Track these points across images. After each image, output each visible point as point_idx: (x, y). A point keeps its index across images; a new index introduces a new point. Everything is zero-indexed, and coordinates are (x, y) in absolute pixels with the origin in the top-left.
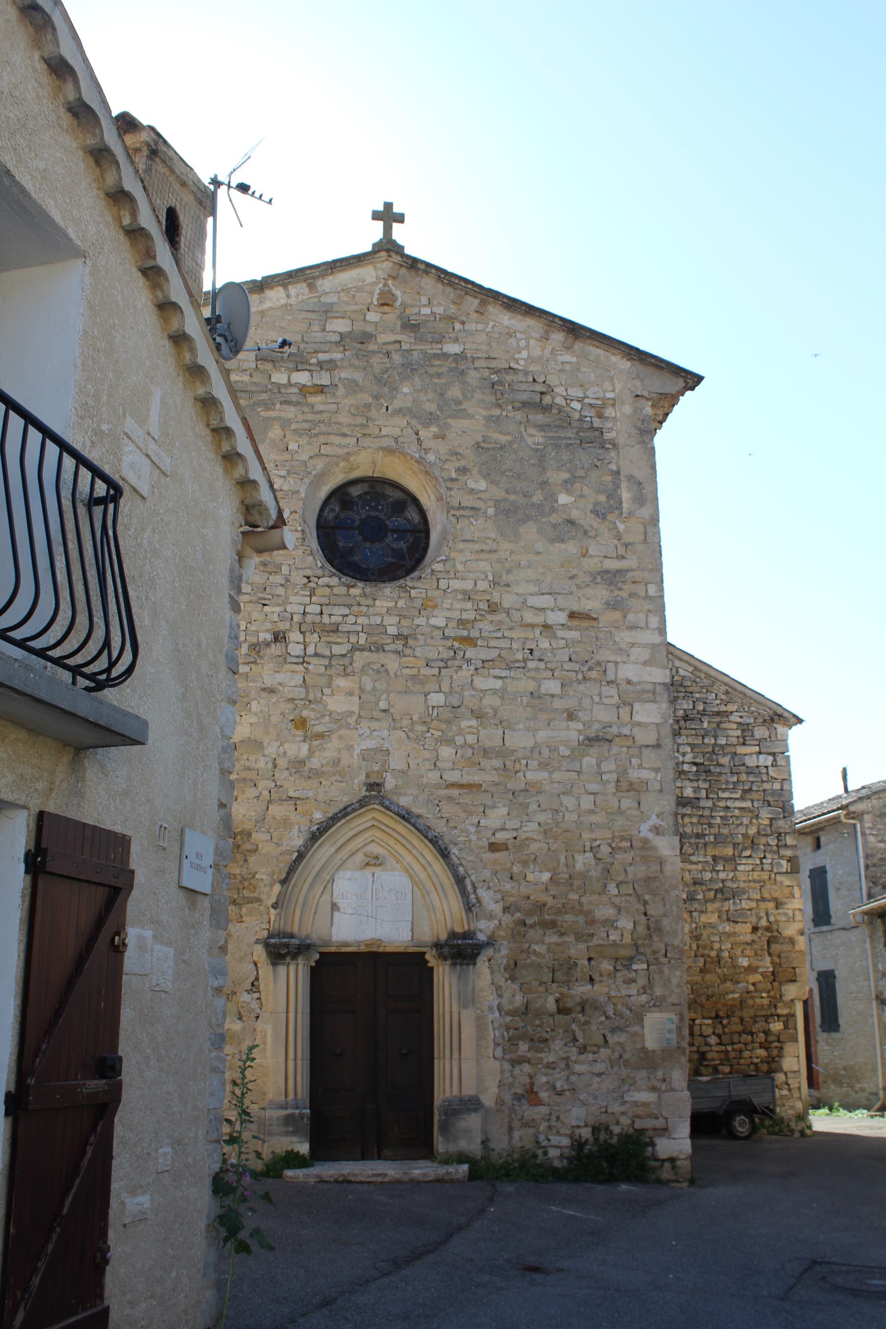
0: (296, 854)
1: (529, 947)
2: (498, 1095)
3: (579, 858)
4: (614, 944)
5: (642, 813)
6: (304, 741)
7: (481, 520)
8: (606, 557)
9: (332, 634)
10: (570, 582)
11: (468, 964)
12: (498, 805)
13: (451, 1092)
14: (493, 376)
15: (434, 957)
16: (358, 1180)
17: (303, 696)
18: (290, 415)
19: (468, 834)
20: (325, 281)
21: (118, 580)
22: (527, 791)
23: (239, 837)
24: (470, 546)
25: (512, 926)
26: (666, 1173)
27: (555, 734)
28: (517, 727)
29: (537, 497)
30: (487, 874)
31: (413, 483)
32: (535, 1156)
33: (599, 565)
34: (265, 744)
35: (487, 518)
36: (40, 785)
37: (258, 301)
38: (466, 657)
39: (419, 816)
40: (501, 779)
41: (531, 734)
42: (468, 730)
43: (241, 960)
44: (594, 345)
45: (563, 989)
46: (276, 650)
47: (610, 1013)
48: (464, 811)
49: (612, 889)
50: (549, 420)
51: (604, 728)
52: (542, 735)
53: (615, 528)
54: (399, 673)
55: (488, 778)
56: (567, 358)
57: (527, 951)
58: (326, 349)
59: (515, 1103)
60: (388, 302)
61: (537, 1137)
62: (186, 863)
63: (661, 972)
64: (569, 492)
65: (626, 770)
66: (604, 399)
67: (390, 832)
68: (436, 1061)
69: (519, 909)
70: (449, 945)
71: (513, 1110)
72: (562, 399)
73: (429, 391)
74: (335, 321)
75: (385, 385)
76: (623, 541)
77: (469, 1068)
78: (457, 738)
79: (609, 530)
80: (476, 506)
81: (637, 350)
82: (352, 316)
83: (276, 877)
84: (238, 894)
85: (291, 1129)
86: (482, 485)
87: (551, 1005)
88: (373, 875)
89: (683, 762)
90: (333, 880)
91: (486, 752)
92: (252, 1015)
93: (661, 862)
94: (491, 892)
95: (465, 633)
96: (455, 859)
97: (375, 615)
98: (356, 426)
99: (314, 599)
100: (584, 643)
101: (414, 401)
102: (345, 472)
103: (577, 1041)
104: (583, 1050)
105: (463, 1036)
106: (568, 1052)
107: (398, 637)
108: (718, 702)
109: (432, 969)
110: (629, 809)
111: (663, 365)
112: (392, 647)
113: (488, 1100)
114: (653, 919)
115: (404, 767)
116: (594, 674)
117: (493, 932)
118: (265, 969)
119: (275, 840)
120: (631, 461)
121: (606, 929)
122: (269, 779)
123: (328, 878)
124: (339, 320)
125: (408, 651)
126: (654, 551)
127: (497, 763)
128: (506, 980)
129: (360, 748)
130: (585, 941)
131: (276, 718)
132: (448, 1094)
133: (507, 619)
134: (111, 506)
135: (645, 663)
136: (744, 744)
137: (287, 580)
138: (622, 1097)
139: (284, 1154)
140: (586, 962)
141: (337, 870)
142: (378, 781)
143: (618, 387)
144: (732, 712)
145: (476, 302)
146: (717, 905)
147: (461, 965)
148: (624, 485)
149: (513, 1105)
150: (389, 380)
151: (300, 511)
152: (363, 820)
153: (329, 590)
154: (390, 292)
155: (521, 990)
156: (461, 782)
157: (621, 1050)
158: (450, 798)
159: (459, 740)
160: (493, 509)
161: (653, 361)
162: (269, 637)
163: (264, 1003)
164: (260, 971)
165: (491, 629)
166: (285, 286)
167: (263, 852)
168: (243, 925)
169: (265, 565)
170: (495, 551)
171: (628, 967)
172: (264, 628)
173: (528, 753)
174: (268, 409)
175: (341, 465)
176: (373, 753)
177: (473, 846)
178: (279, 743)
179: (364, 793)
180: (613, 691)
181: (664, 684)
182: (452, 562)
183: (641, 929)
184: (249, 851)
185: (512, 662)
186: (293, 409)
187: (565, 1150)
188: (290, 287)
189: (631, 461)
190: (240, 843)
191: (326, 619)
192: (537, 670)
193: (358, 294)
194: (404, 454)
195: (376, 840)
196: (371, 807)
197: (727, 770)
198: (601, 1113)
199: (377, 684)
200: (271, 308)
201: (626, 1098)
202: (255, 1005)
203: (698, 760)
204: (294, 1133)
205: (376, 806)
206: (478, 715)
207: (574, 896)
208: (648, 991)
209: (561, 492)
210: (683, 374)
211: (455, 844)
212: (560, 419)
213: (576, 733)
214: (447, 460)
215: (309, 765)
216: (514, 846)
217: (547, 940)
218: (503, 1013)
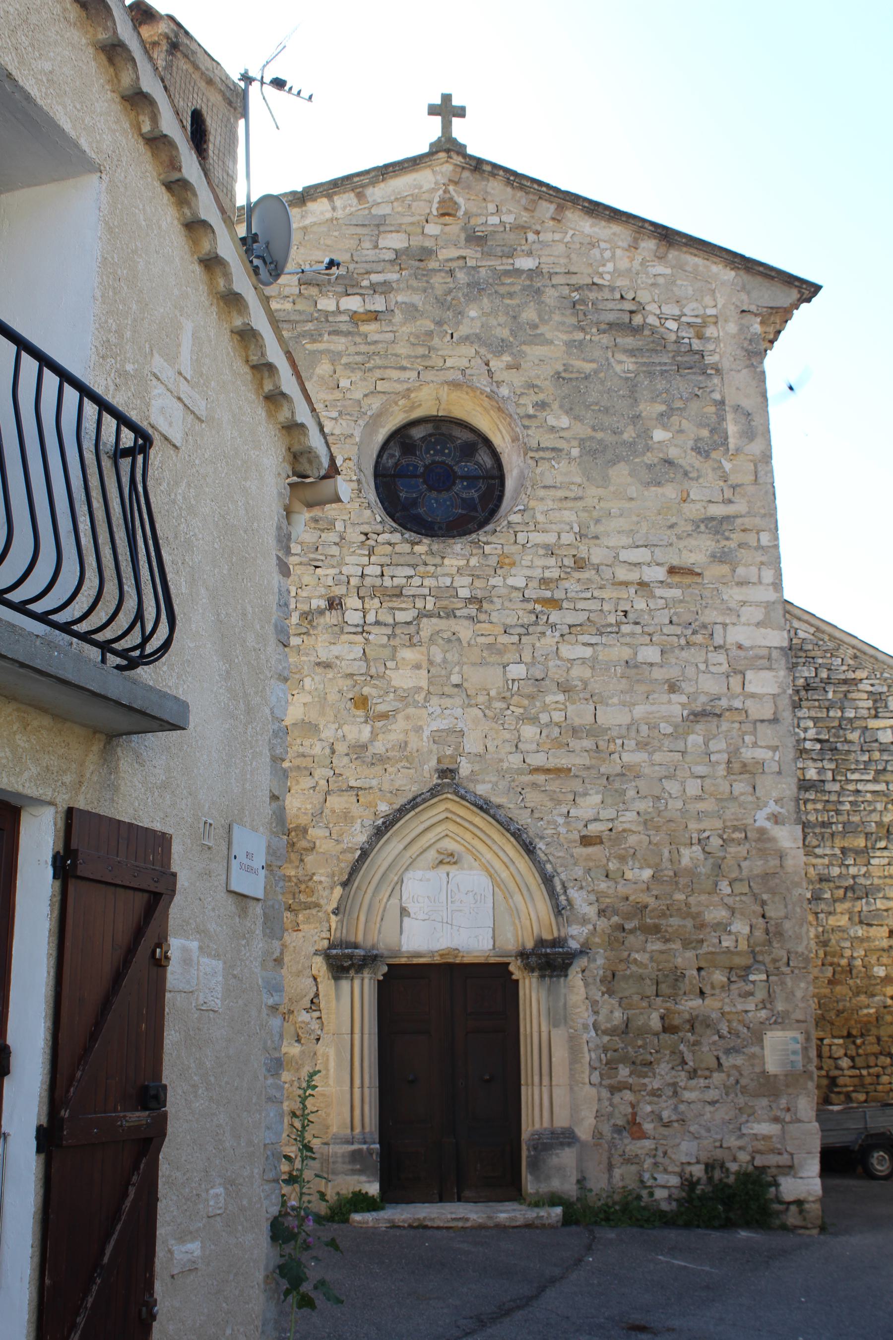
0: (359, 852)
1: (629, 955)
2: (595, 1127)
3: (686, 852)
4: (728, 951)
5: (758, 798)
6: (366, 722)
7: (564, 463)
8: (710, 501)
9: (394, 599)
10: (669, 532)
11: (559, 976)
12: (591, 792)
13: (542, 1124)
14: (573, 294)
15: (519, 968)
16: (435, 1225)
17: (363, 671)
18: (341, 348)
19: (557, 826)
20: (376, 189)
21: (151, 542)
22: (623, 775)
23: (293, 834)
24: (552, 492)
26: (792, 1218)
27: (654, 708)
28: (610, 702)
29: (629, 434)
30: (579, 872)
31: (484, 423)
32: (639, 1198)
33: (703, 510)
34: (321, 727)
35: (571, 460)
36: (68, 779)
37: (299, 216)
38: (550, 621)
39: (499, 806)
40: (594, 762)
41: (627, 709)
42: (553, 706)
43: (299, 974)
44: (691, 254)
45: (668, 1004)
46: (331, 618)
47: (724, 1031)
48: (552, 799)
49: (725, 887)
50: (640, 343)
51: (712, 701)
52: (639, 711)
53: (721, 467)
54: (473, 642)
55: (578, 761)
56: (660, 269)
57: (627, 960)
58: (380, 269)
59: (615, 1136)
60: (450, 211)
61: (641, 1176)
62: (234, 864)
63: (783, 983)
64: (665, 427)
65: (738, 749)
66: (705, 317)
67: (466, 825)
68: (523, 1089)
69: (616, 912)
71: (612, 1145)
72: (655, 318)
73: (500, 314)
74: (389, 236)
75: (449, 309)
76: (730, 483)
77: (561, 1095)
78: (541, 715)
79: (714, 469)
80: (558, 446)
81: (742, 257)
82: (409, 229)
83: (336, 878)
84: (294, 898)
86: (564, 421)
87: (655, 1022)
88: (448, 875)
89: (805, 739)
90: (402, 881)
91: (575, 731)
92: (312, 1037)
93: (781, 856)
94: (584, 893)
95: (548, 594)
96: (542, 855)
97: (444, 575)
98: (417, 357)
99: (373, 559)
100: (687, 602)
101: (482, 326)
102: (404, 412)
103: (686, 1064)
104: (693, 1074)
105: (554, 1059)
106: (676, 1077)
107: (472, 600)
108: (845, 668)
109: (517, 981)
110: (742, 794)
111: (773, 274)
112: (465, 612)
113: (584, 1132)
114: (773, 922)
115: (481, 750)
116: (699, 638)
117: (587, 939)
118: (326, 985)
119: (334, 836)
120: (738, 389)
121: (717, 934)
123: (396, 879)
124: (394, 235)
125: (482, 617)
126: (766, 492)
127: (588, 743)
128: (603, 994)
129: (430, 729)
130: (694, 948)
131: (332, 697)
132: (537, 1126)
133: (596, 577)
134: (140, 458)
135: (758, 625)
136: (876, 716)
137: (342, 538)
138: (740, 1129)
139: (351, 1195)
140: (695, 973)
141: (407, 869)
142: (451, 767)
143: (721, 302)
144: (861, 680)
145: (552, 207)
146: (847, 905)
147: (551, 977)
148: (730, 417)
149: (613, 1138)
150: (454, 302)
151: (355, 458)
152: (435, 812)
153: (390, 548)
154: (451, 199)
155: (620, 1005)
156: (548, 766)
157: (737, 1074)
158: (535, 785)
159: (544, 718)
160: (578, 449)
161: (761, 269)
162: (323, 604)
163: (325, 1023)
164: (320, 986)
165: (578, 589)
166: (330, 197)
167: (321, 850)
168: (301, 934)
169: (316, 520)
170: (581, 498)
171: (744, 978)
172: (317, 594)
173: (624, 732)
174: (314, 341)
175: (400, 403)
176: (445, 734)
177: (562, 839)
178: (337, 726)
180: (721, 658)
181: (781, 648)
182: (531, 512)
183: (759, 934)
184: (305, 849)
185: (603, 626)
186: (343, 340)
187: (673, 1190)
188: (336, 198)
189: (738, 389)
190: (295, 840)
191: (387, 582)
192: (632, 634)
193: (415, 204)
194: (473, 388)
195: (451, 834)
196: (444, 796)
197: (856, 748)
198: (716, 1147)
199: (447, 655)
200: (315, 224)
201: (744, 1131)
202: (315, 1025)
203: (822, 737)
204: (361, 1172)
205: (449, 796)
206: (565, 688)
207: (680, 897)
208: (768, 1006)
209: (656, 427)
210: (797, 283)
211: (542, 838)
212: (653, 342)
213: (679, 707)
214: (522, 394)
215: (371, 750)
216: (610, 839)
217: (650, 947)
218: (599, 1032)
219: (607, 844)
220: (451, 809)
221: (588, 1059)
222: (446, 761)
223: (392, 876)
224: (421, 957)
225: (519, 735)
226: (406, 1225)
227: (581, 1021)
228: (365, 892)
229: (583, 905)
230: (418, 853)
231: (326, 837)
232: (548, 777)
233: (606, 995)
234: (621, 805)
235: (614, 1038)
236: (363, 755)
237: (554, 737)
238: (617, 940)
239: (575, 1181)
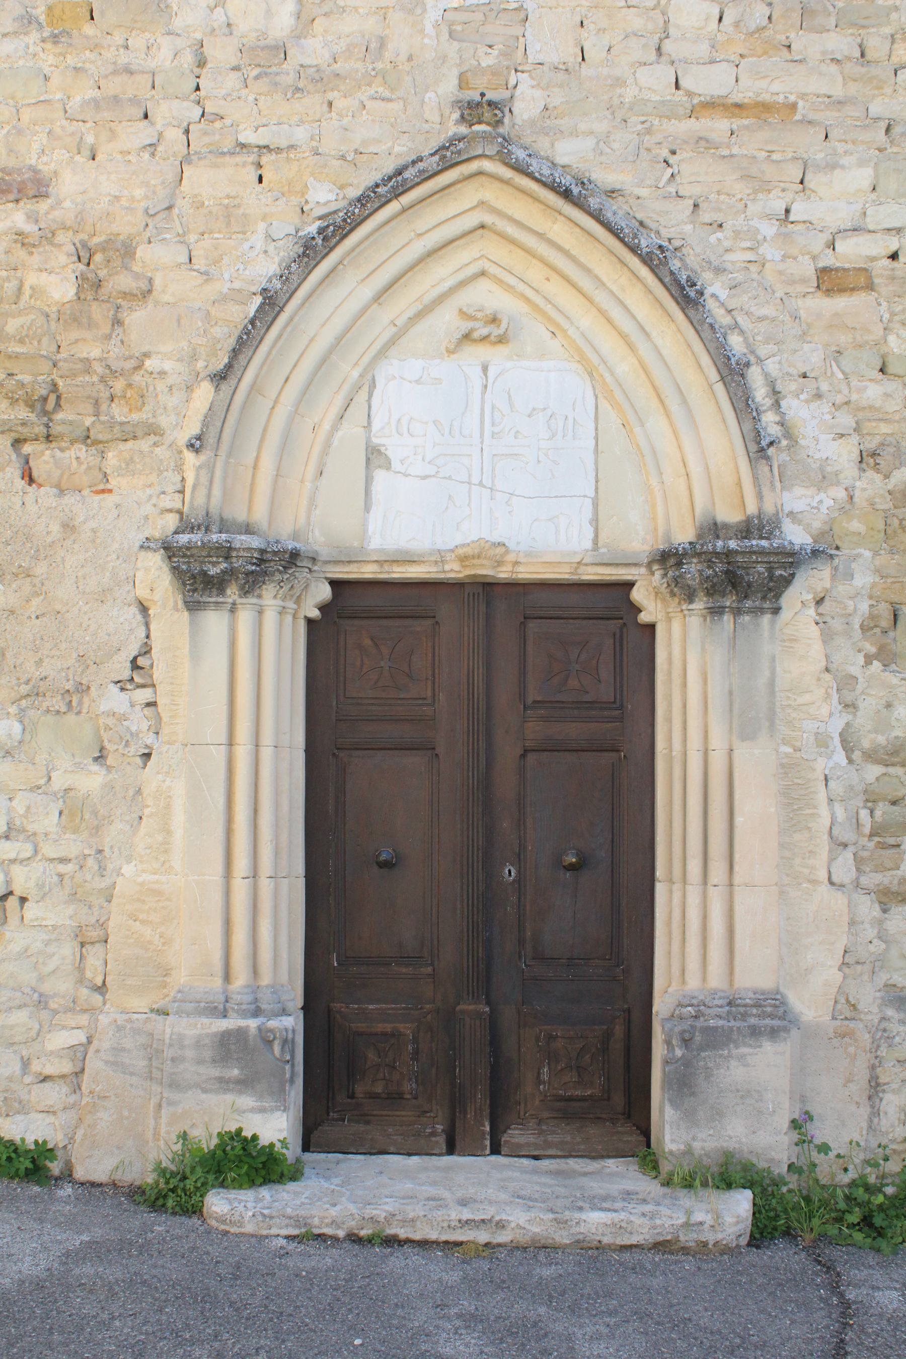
0: (258, 300)
12: (845, 161)
13: (704, 979)
16: (417, 1237)
23: (98, 258)
25: (885, 504)
39: (611, 193)
40: (853, 89)
43: (102, 596)
48: (747, 177)
55: (815, 85)
59: (890, 1012)
67: (531, 241)
68: (660, 889)
70: (699, 555)
83: (200, 364)
84: (97, 415)
85: (236, 1072)
88: (485, 369)
90: (373, 385)
92: (132, 750)
105: (739, 820)
109: (651, 628)
115: (571, 54)
119: (200, 263)
122: (185, 98)
123: (355, 374)
128: (868, 660)
132: (693, 983)
139: (215, 1141)
141: (382, 353)
147: (737, 612)
149: (883, 1019)
152: (452, 208)
156: (737, 98)
158: (704, 143)
163: (165, 719)
164: (152, 627)
167: (167, 298)
168: (110, 500)
176: (479, 16)
179: (454, 128)
184: (125, 295)
190: (102, 274)
195: (493, 269)
196: (474, 166)
202: (139, 722)
204: (244, 1084)
205: (487, 165)
211: (719, 270)
215: (296, 57)
218: (857, 755)
219: (884, 291)
220: (499, 204)
221: (828, 823)
222: (480, 83)
225: (666, 22)
226: (341, 1234)
227: (810, 726)
228: (276, 402)
229: (823, 437)
230: (410, 313)
231: (179, 265)
232: (736, 123)
233: (876, 664)
235: (891, 770)
236: (274, 69)
237: (753, 26)
239: (785, 1124)
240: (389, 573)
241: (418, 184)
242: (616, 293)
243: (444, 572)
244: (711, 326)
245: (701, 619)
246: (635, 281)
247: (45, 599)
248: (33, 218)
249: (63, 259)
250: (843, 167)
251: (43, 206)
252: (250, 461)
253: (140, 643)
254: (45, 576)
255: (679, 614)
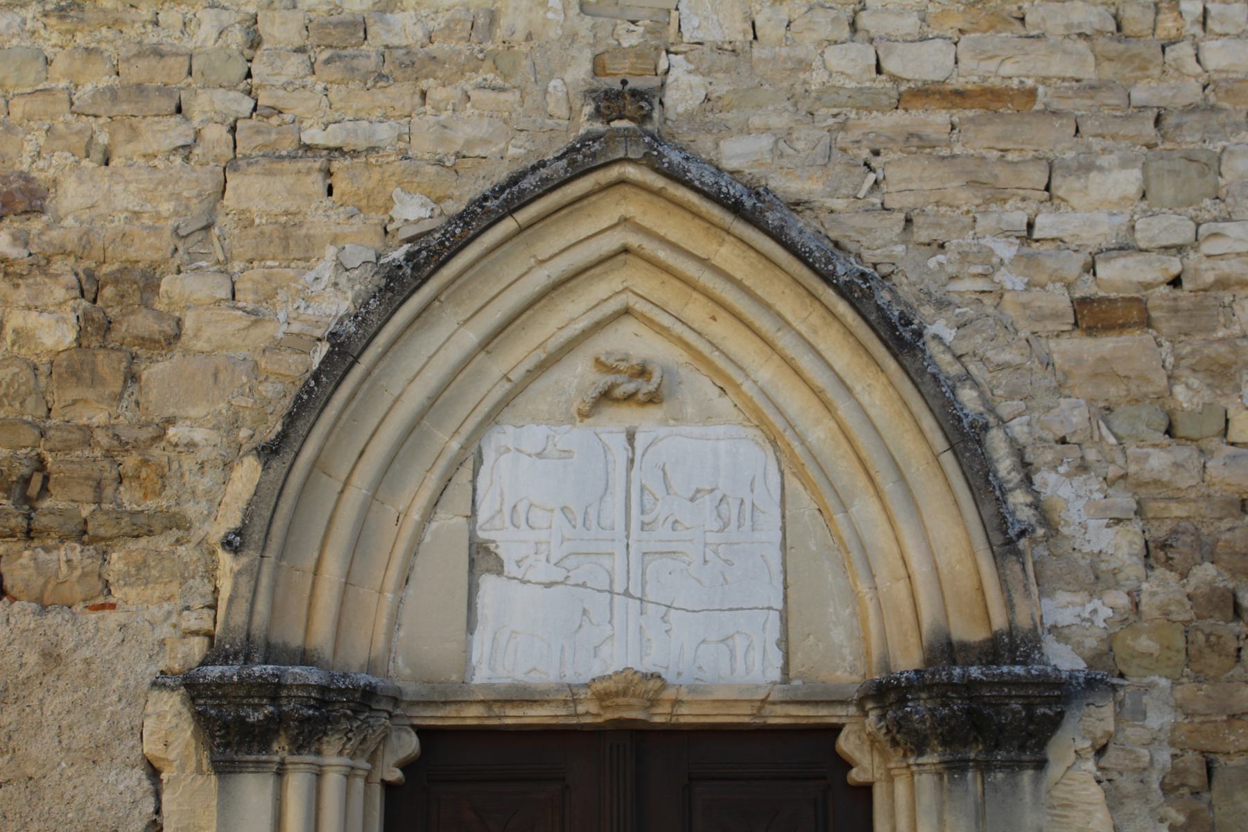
0: (324, 348)
11: (1014, 766)
12: (1104, 161)
15: (873, 742)
23: (108, 292)
25: (1184, 613)
39: (796, 205)
40: (1108, 70)
43: (96, 755)
48: (973, 183)
55: (1058, 66)
70: (929, 687)
83: (244, 433)
84: (98, 501)
88: (631, 437)
90: (479, 460)
109: (866, 791)
115: (737, 32)
117: (1110, 640)
119: (246, 299)
123: (455, 445)
141: (492, 418)
147: (985, 767)
152: (585, 227)
156: (957, 83)
158: (917, 143)
164: (165, 797)
167: (200, 345)
168: (112, 619)
177: (1010, 309)
179: (585, 125)
184: (144, 341)
190: (113, 312)
195: (640, 306)
196: (614, 173)
205: (631, 172)
211: (942, 304)
215: (379, 36)
216: (1175, 310)
219: (1165, 327)
220: (648, 221)
222: (622, 67)
223: (442, 436)
224: (533, 702)
228: (346, 484)
229: (1092, 523)
230: (529, 364)
232: (957, 116)
234: (1207, 202)
236: (350, 51)
238: (1214, 643)
240: (500, 717)
241: (539, 196)
242: (806, 335)
243: (577, 715)
244: (935, 377)
245: (936, 778)
246: (829, 319)
247: (12, 759)
248: (21, 239)
249: (60, 293)
250: (1101, 169)
251: (36, 225)
252: (310, 564)
253: (146, 821)
254: (11, 727)
255: (905, 771)
